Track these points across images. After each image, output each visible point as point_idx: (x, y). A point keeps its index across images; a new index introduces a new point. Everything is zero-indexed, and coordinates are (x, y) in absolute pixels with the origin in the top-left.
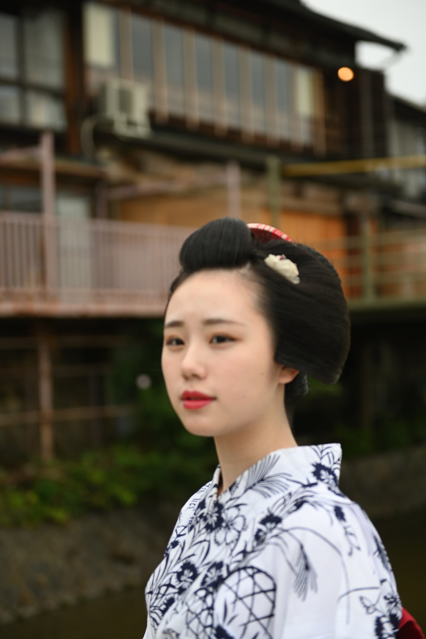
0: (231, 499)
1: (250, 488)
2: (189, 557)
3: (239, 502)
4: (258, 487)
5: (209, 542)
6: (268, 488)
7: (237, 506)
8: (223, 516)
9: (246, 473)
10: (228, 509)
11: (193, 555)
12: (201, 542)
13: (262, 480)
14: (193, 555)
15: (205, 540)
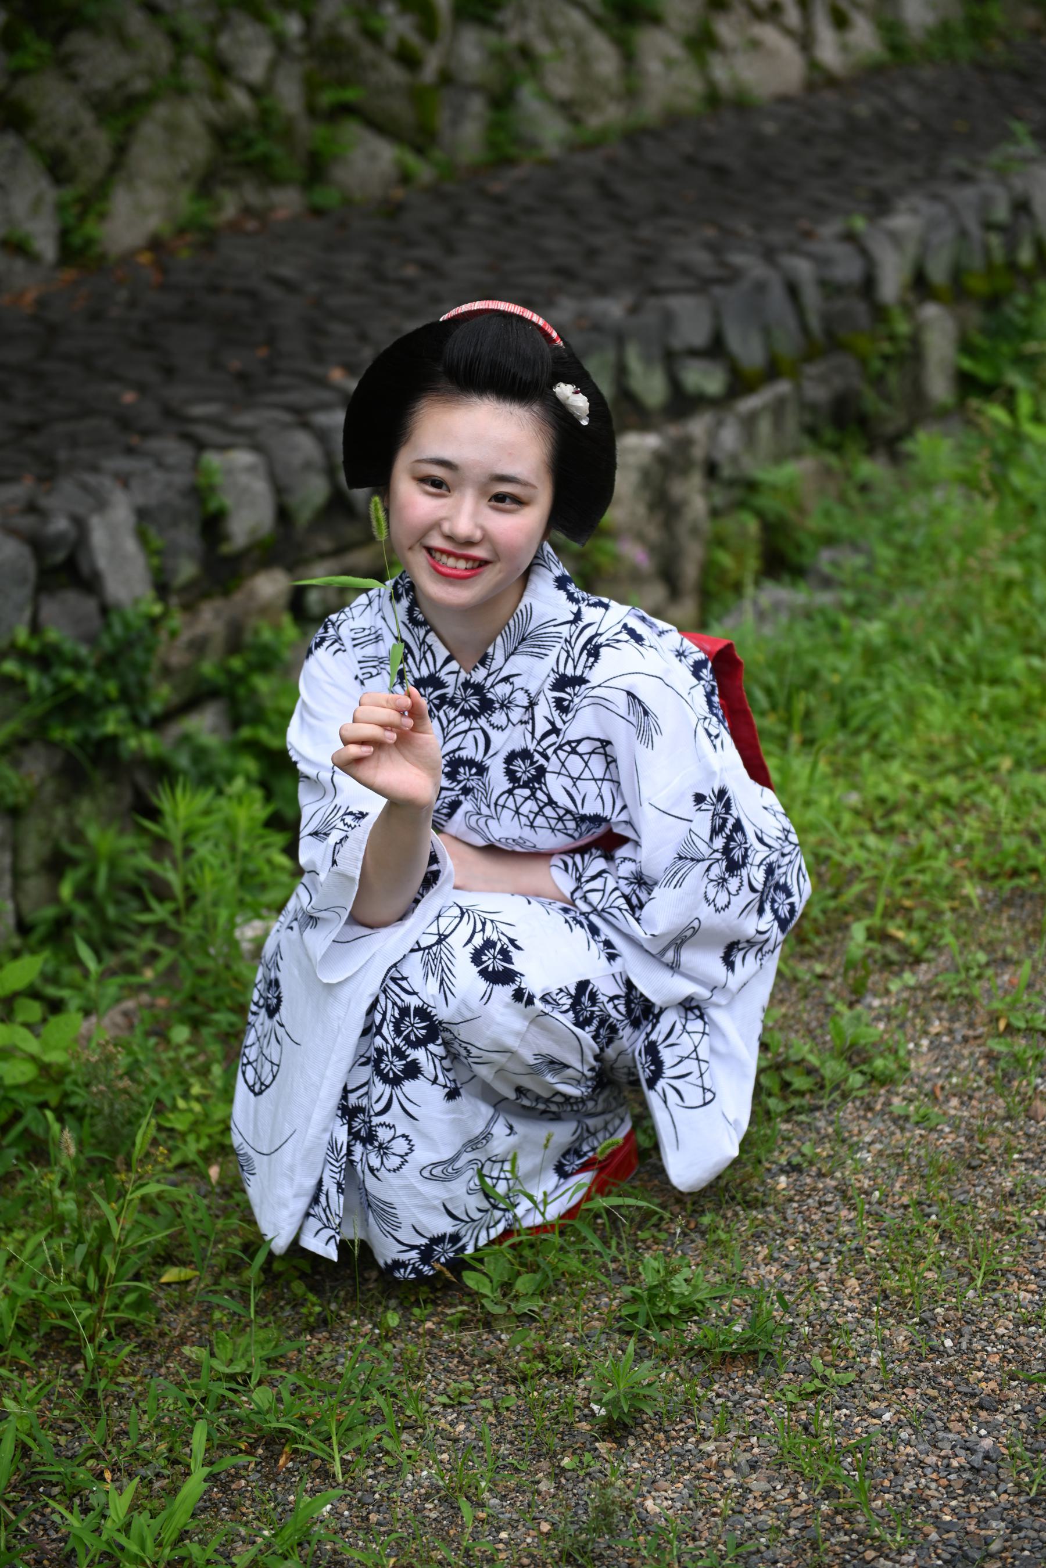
0: (489, 675)
1: (513, 654)
2: (454, 752)
3: (504, 674)
4: (521, 648)
5: (482, 729)
6: (539, 647)
7: (506, 679)
8: (490, 696)
9: (499, 640)
10: (492, 686)
11: (459, 749)
12: (466, 732)
13: (524, 639)
14: (459, 749)
15: (470, 729)
